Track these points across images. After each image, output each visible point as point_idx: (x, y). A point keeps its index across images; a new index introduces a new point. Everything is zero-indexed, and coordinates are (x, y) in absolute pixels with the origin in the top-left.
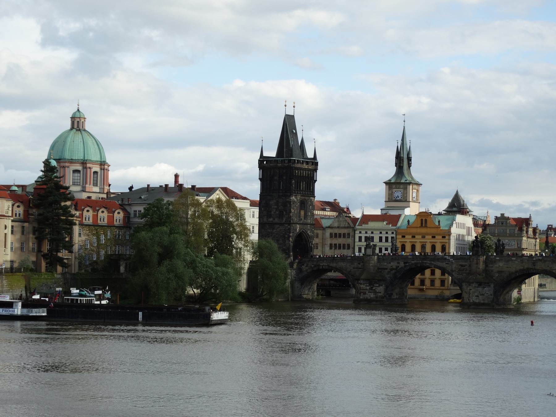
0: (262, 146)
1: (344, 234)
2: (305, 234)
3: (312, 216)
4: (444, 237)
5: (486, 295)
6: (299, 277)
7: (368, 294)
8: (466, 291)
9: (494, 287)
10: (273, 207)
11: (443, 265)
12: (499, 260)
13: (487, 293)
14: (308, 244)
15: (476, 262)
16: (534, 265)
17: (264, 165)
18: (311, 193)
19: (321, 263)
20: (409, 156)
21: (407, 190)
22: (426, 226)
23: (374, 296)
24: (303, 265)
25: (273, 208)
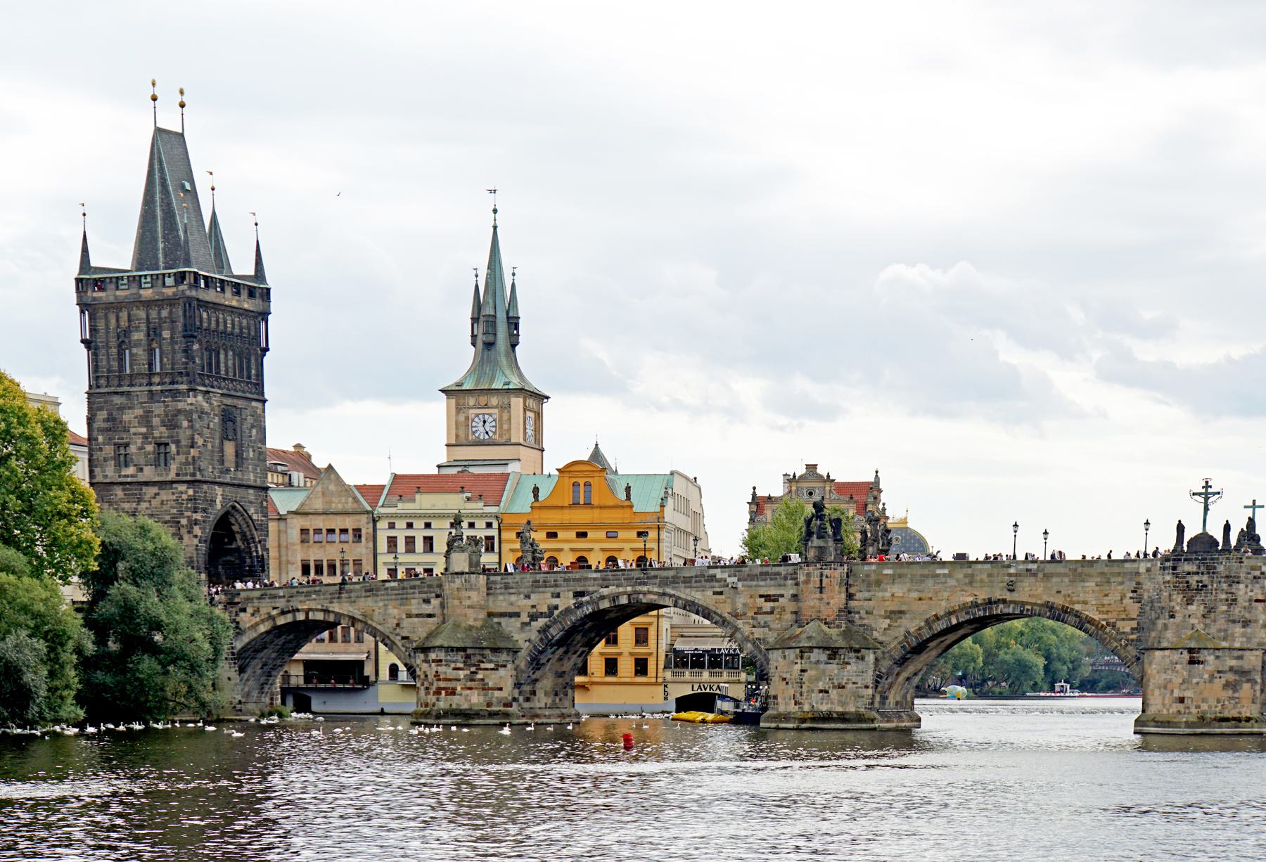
2: (242, 515)
3: (259, 459)
5: (850, 686)
8: (788, 676)
11: (704, 597)
12: (893, 579)
14: (253, 549)
15: (818, 585)
16: (1012, 591)
19: (301, 602)
21: (509, 412)
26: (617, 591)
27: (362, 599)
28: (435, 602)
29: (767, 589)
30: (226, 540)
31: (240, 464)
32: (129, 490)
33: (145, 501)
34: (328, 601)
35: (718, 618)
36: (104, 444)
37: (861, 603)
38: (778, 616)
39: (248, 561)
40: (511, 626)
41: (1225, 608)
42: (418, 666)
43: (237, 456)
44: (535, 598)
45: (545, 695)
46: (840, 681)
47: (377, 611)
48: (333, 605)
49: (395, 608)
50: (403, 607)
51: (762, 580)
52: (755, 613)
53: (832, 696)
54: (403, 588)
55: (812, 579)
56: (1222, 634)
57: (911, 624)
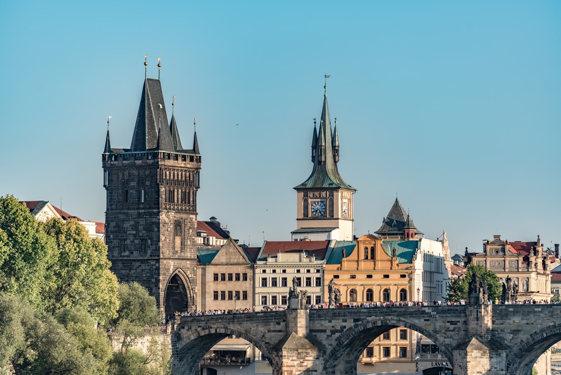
0: (108, 131)
3: (193, 245)
4: (403, 276)
6: (177, 348)
8: (461, 364)
10: (128, 232)
13: (495, 367)
14: (188, 293)
17: (112, 163)
18: (191, 208)
19: (213, 323)
22: (373, 258)
24: (184, 328)
25: (129, 234)
26: (376, 318)
27: (245, 322)
28: (283, 324)
29: (451, 318)
30: (174, 288)
31: (183, 248)
32: (125, 263)
33: (134, 270)
34: (227, 323)
35: (427, 333)
36: (113, 239)
38: (457, 332)
39: (185, 299)
42: (273, 358)
43: (182, 244)
44: (334, 322)
45: (340, 374)
47: (253, 329)
48: (230, 325)
49: (262, 327)
50: (266, 327)
51: (449, 314)
52: (446, 331)
54: (266, 317)
57: (523, 337)
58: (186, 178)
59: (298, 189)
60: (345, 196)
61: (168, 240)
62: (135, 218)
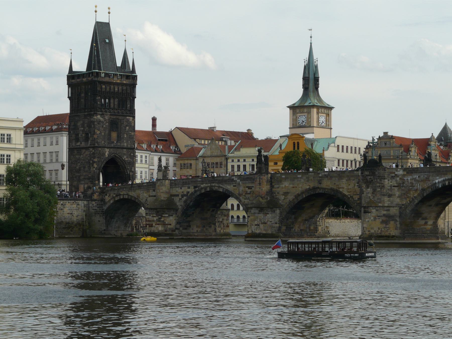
0: (71, 59)
1: (217, 163)
2: (120, 159)
5: (269, 223)
6: (103, 209)
7: (155, 227)
9: (281, 213)
11: (230, 187)
14: (126, 172)
15: (259, 183)
16: (320, 183)
19: (121, 191)
20: (315, 76)
21: (311, 114)
23: (163, 229)
24: (106, 195)
25: (80, 130)
33: (82, 155)
37: (276, 189)
40: (176, 199)
41: (379, 189)
46: (264, 221)
47: (141, 194)
48: (130, 192)
52: (245, 194)
53: (261, 227)
54: (148, 186)
55: (257, 180)
56: (379, 200)
57: (291, 197)
58: (123, 90)
59: (290, 107)
60: (323, 112)
61: (103, 134)
62: (83, 119)
